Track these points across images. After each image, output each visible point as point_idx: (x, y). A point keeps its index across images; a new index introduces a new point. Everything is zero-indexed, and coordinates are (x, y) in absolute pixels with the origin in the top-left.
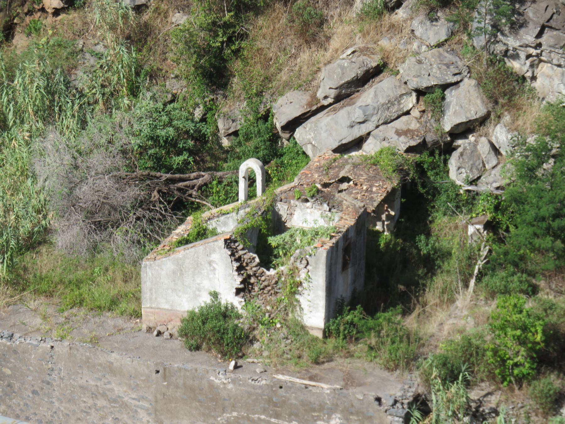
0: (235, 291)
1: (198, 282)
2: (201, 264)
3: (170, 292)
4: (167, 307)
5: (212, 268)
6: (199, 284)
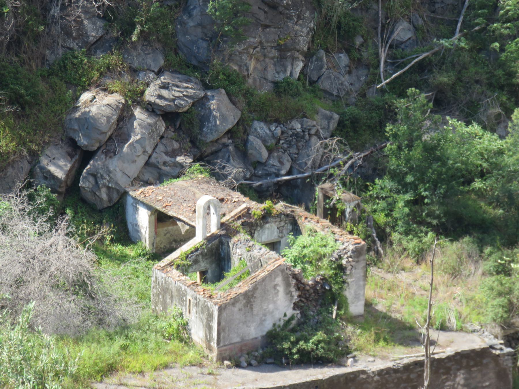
0: (292, 305)
1: (265, 308)
2: (268, 291)
3: (241, 325)
4: (237, 340)
5: (276, 291)
6: (265, 310)
